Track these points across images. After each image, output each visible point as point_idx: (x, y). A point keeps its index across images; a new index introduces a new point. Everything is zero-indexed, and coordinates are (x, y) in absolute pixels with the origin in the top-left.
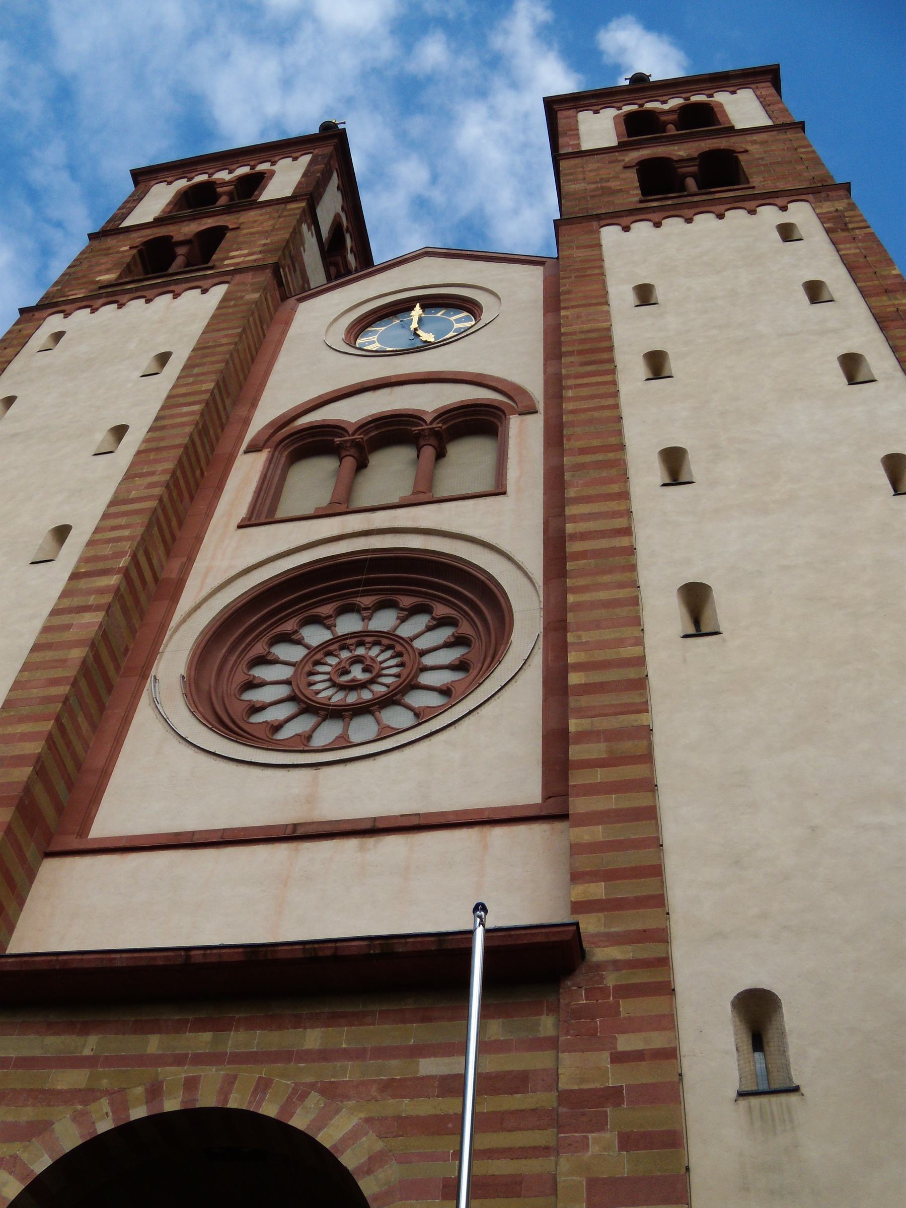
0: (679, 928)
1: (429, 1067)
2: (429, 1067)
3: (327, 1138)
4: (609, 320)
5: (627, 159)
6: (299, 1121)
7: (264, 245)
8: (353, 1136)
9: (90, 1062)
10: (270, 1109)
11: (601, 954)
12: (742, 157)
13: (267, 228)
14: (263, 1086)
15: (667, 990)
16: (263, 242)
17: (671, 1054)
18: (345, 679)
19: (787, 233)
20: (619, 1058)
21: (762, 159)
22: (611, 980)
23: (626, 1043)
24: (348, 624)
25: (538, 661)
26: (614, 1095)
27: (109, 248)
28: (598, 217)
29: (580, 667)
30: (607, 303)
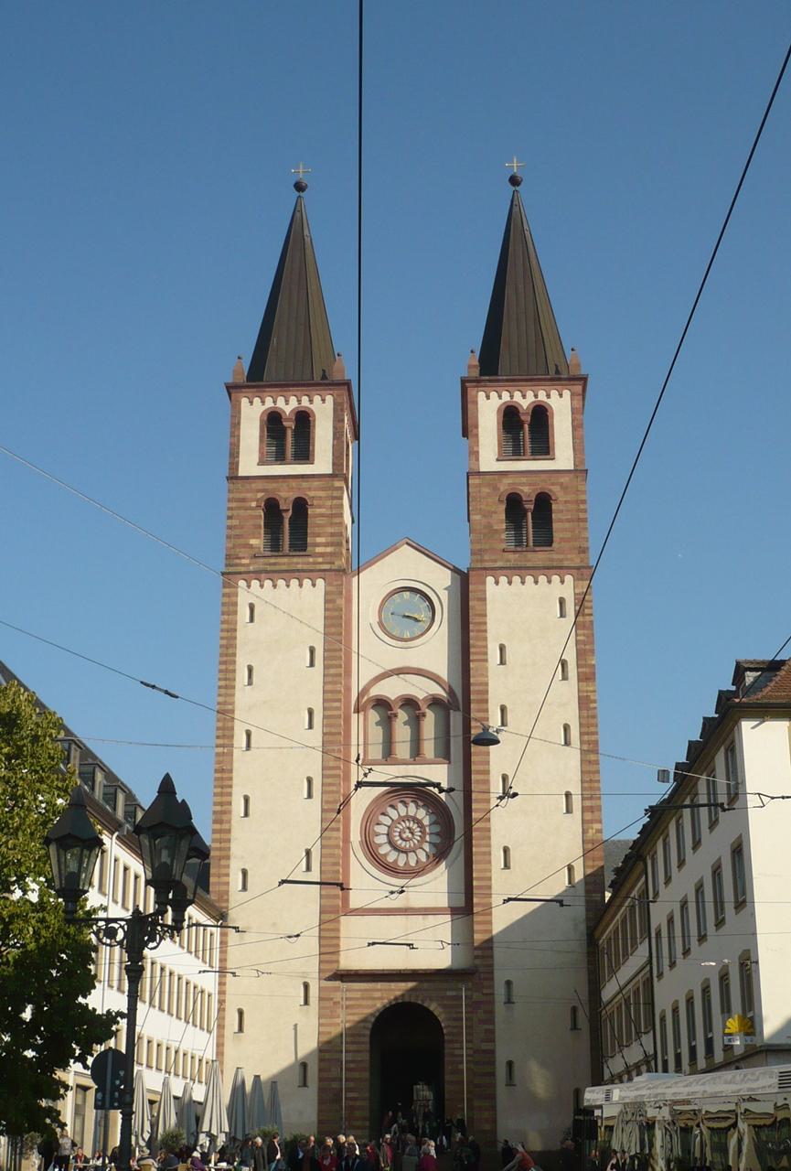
0: (495, 967)
1: (449, 993)
2: (449, 993)
3: (431, 1008)
4: (487, 677)
5: (502, 489)
6: (426, 1005)
7: (332, 535)
8: (436, 1008)
9: (381, 990)
10: (420, 1002)
11: (481, 969)
12: (554, 507)
13: (329, 512)
14: (417, 996)
15: (492, 979)
16: (330, 530)
17: (493, 994)
18: (410, 835)
19: (562, 601)
20: (483, 994)
21: (562, 511)
22: (482, 976)
23: (485, 991)
24: (402, 810)
25: (463, 852)
26: (481, 1002)
27: (244, 500)
28: (485, 569)
29: (478, 879)
30: (486, 661)
